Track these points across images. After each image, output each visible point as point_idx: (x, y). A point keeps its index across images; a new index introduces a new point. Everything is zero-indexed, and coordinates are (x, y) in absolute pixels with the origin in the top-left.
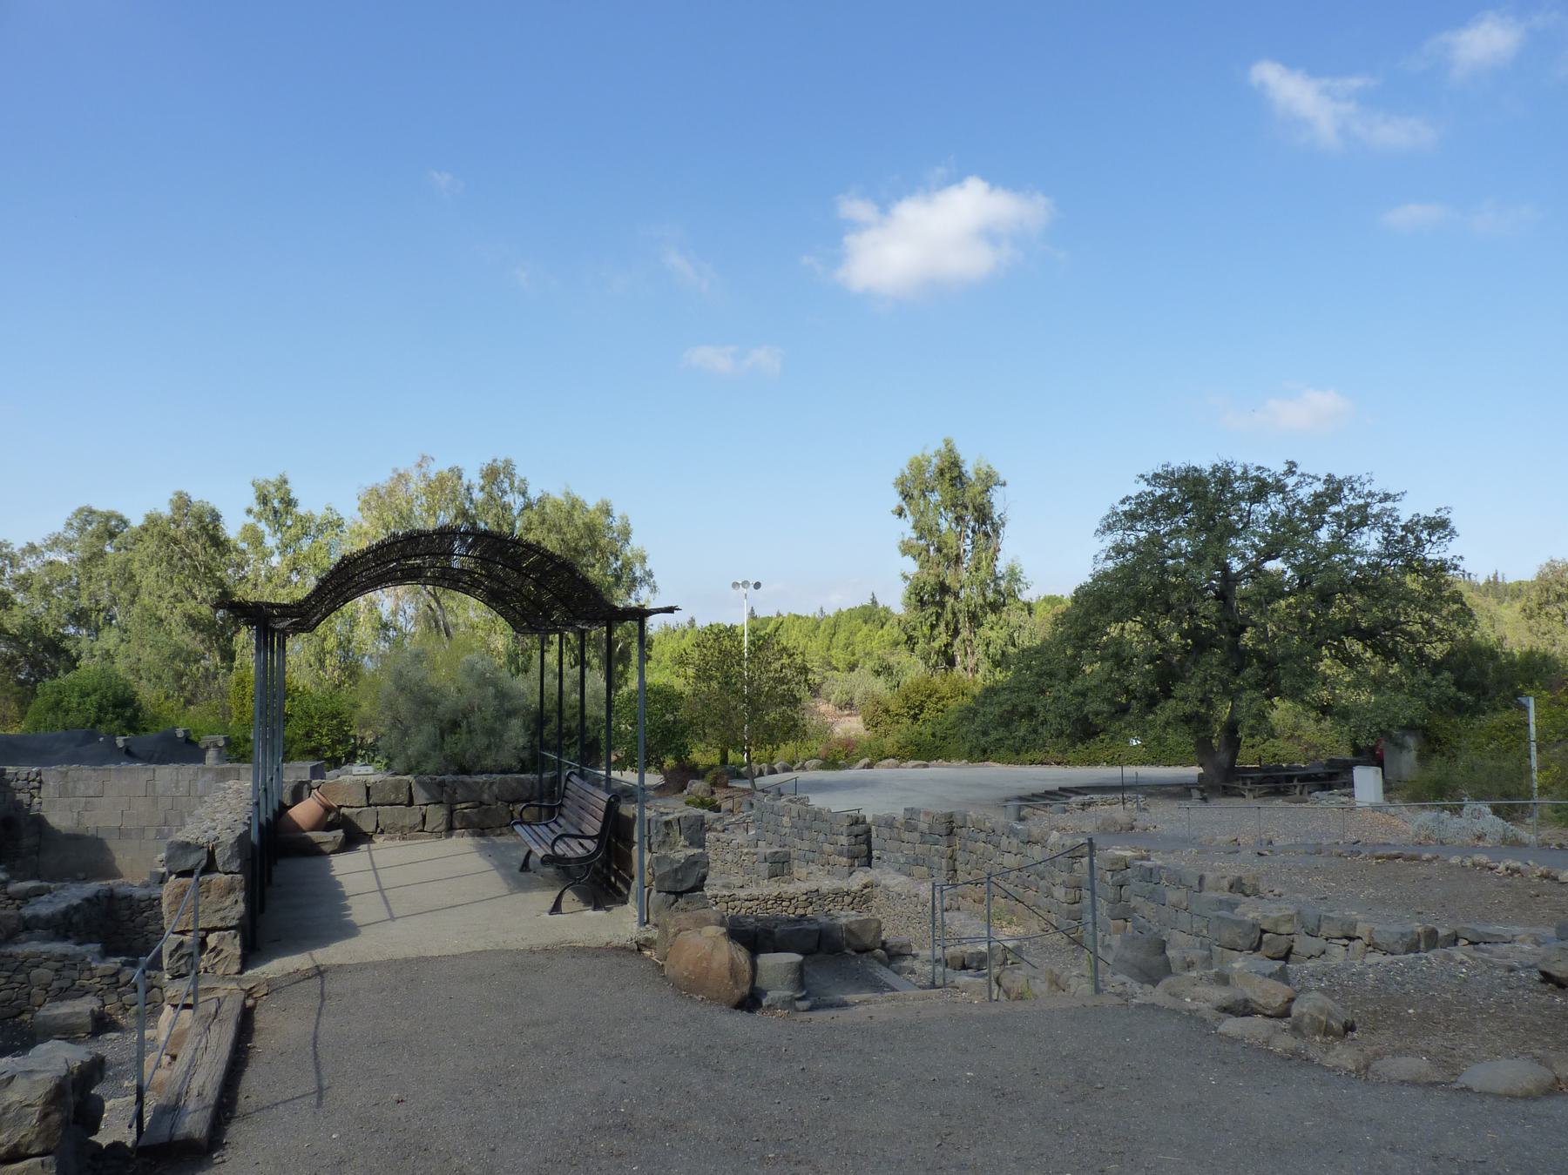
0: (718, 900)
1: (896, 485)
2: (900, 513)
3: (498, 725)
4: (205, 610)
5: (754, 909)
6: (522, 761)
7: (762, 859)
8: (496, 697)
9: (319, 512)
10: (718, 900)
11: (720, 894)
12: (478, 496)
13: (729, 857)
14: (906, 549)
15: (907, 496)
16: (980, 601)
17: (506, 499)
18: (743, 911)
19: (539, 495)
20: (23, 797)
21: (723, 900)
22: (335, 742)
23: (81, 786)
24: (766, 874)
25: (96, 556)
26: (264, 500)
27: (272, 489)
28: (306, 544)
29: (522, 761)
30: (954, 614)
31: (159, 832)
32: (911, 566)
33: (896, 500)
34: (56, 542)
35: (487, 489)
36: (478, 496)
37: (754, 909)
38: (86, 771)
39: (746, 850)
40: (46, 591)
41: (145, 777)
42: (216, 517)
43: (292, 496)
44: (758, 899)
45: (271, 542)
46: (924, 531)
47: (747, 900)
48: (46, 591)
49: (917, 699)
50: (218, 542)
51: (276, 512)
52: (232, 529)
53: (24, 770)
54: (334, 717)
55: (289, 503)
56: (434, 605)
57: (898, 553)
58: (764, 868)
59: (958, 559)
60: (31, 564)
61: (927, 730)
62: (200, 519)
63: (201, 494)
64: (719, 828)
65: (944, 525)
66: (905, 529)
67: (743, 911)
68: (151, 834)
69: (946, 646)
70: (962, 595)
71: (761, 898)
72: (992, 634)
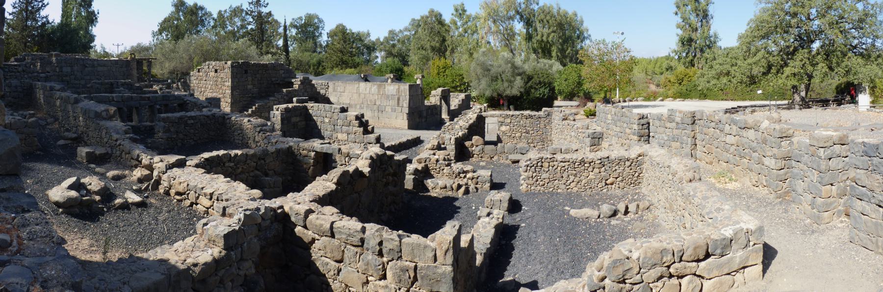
0: (543, 160)
1: (675, 4)
2: (676, 14)
3: (512, 79)
4: (438, 45)
5: (566, 167)
6: (521, 92)
7: (587, 136)
8: (511, 68)
9: (474, 14)
10: (543, 160)
11: (545, 157)
12: (523, 6)
13: (573, 134)
14: (678, 26)
15: (678, 7)
16: (704, 44)
17: (531, 7)
18: (559, 168)
19: (543, 5)
20: (322, 92)
21: (546, 160)
22: (461, 85)
23: (339, 88)
24: (588, 144)
25: (416, 32)
26: (457, 10)
27: (459, 7)
28: (469, 24)
29: (521, 92)
30: (695, 49)
31: (360, 106)
32: (680, 32)
33: (675, 9)
34: (406, 29)
35: (526, 3)
36: (523, 6)
37: (566, 167)
38: (340, 83)
39: (580, 131)
40: (403, 42)
41: (357, 86)
42: (441, 15)
43: (465, 9)
44: (569, 162)
45: (459, 24)
46: (684, 19)
47: (562, 162)
48: (403, 42)
49: (681, 76)
50: (441, 23)
51: (460, 14)
52: (447, 18)
53: (320, 82)
54: (461, 75)
55: (464, 11)
56: (507, 42)
57: (675, 27)
58: (588, 141)
59: (697, 30)
60: (400, 35)
61: (684, 88)
62: (436, 16)
63: (437, 9)
64: (572, 119)
65: (692, 18)
66: (678, 19)
67: (559, 168)
68: (358, 107)
69: (692, 60)
70: (698, 42)
71: (571, 161)
72: (708, 56)
